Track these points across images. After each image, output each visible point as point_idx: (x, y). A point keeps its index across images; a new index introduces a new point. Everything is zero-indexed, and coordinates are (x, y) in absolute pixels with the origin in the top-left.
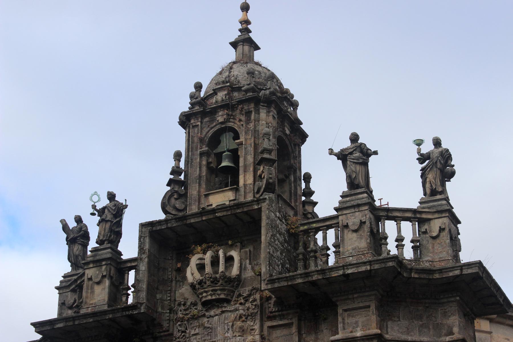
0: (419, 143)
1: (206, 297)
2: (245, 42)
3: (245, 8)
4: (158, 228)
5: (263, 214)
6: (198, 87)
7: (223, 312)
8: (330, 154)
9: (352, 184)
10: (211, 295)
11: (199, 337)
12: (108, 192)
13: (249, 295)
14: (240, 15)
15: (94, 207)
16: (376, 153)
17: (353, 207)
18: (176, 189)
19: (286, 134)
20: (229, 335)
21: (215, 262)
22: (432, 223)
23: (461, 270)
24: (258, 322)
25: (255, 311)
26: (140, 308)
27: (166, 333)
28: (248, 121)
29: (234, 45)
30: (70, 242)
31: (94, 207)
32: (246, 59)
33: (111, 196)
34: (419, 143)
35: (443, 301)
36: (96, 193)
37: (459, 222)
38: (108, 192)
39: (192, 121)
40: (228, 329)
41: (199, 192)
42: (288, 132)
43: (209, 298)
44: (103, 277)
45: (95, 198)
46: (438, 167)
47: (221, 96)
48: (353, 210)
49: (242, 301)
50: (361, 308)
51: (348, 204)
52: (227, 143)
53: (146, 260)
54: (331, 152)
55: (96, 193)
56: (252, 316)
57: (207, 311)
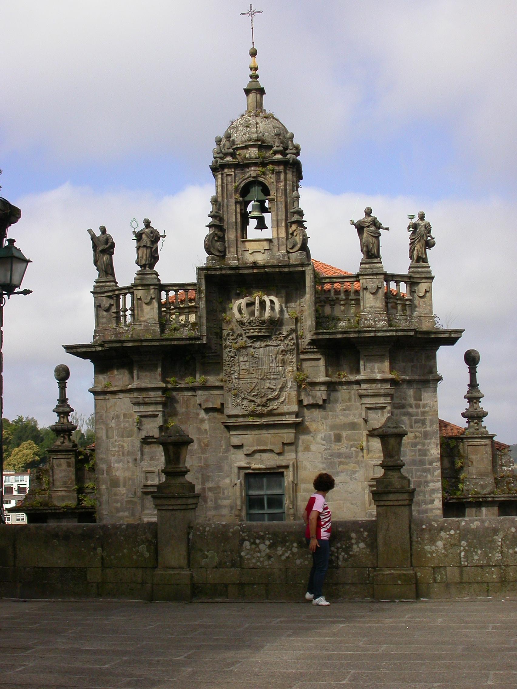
1: (253, 333)
2: (255, 90)
3: (254, 54)
4: (213, 273)
5: (307, 276)
7: (267, 346)
10: (258, 332)
11: (247, 363)
12: (145, 220)
13: (288, 336)
17: (373, 275)
18: (216, 232)
20: (274, 365)
22: (420, 285)
23: (450, 334)
25: (293, 347)
26: (202, 340)
27: (213, 354)
28: (278, 181)
29: (247, 92)
30: (95, 247)
31: (134, 233)
32: (258, 109)
33: (147, 224)
38: (145, 220)
40: (273, 360)
41: (236, 236)
43: (256, 334)
47: (253, 152)
48: (372, 277)
49: (282, 338)
50: (378, 355)
51: (368, 272)
53: (204, 299)
54: (353, 223)
56: (291, 351)
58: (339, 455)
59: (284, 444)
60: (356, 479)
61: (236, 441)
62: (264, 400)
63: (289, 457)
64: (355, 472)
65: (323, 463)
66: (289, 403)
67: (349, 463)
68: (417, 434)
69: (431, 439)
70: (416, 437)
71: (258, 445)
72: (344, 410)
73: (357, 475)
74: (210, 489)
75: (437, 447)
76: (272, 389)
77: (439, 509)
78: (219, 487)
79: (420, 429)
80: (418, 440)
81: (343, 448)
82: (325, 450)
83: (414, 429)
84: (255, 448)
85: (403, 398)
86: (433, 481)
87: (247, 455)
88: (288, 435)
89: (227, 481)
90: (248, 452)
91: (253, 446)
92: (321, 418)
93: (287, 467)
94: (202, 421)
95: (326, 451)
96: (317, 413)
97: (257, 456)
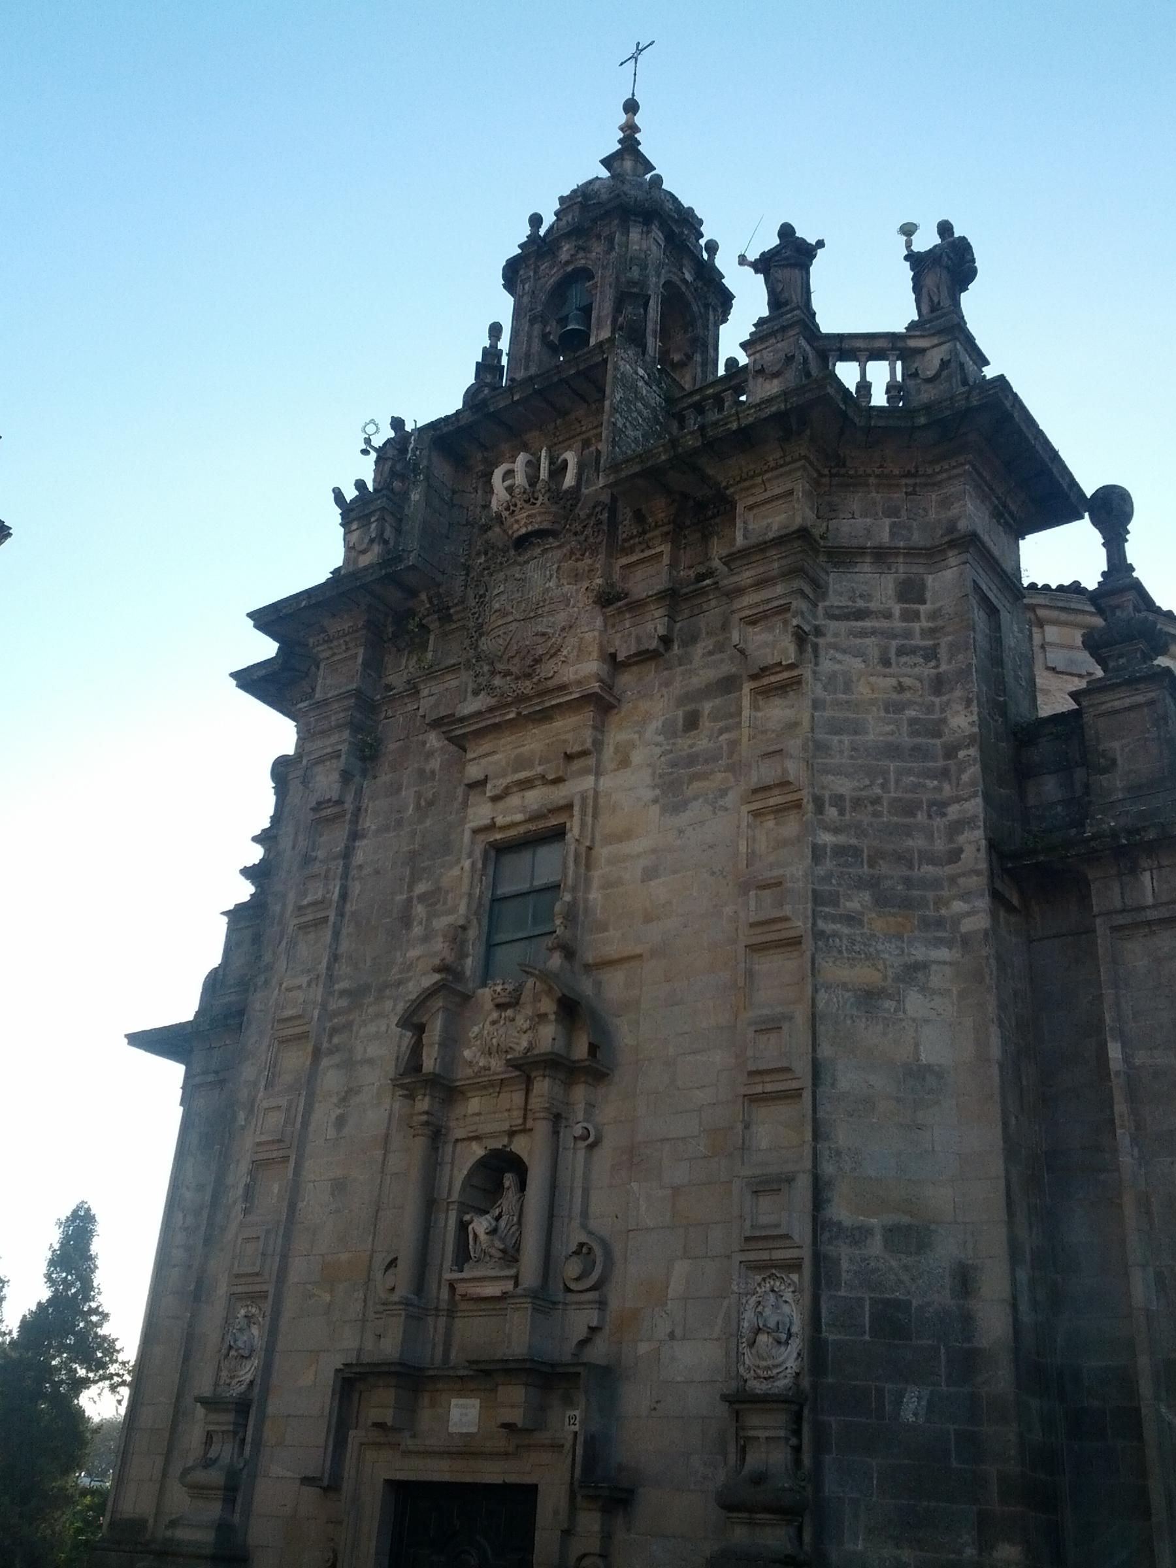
0: (908, 230)
3: (631, 107)
6: (536, 220)
8: (741, 264)
9: (775, 302)
11: (504, 597)
14: (622, 118)
15: (368, 441)
16: (821, 244)
19: (684, 281)
21: (533, 465)
24: (602, 557)
25: (599, 540)
31: (368, 441)
34: (908, 230)
35: (939, 478)
36: (372, 421)
37: (987, 363)
39: (521, 272)
40: (551, 576)
42: (689, 277)
43: (523, 531)
44: (372, 541)
45: (371, 429)
46: (944, 268)
52: (576, 296)
55: (372, 421)
57: (519, 555)
58: (692, 760)
59: (569, 757)
60: (726, 809)
61: (474, 772)
62: (529, 662)
63: (579, 786)
64: (723, 793)
65: (654, 787)
66: (579, 659)
67: (712, 772)
68: (907, 681)
69: (952, 690)
70: (900, 688)
71: (516, 771)
72: (711, 653)
73: (731, 798)
74: (422, 898)
75: (968, 706)
76: (544, 634)
77: (978, 873)
78: (439, 889)
79: (917, 670)
80: (908, 695)
81: (702, 742)
82: (663, 754)
83: (894, 669)
84: (509, 780)
85: (861, 596)
86: (958, 800)
87: (495, 799)
88: (571, 729)
89: (456, 872)
90: (497, 792)
91: (504, 775)
92: (660, 685)
93: (569, 807)
94: (430, 754)
95: (662, 759)
96: (651, 674)
97: (514, 800)
